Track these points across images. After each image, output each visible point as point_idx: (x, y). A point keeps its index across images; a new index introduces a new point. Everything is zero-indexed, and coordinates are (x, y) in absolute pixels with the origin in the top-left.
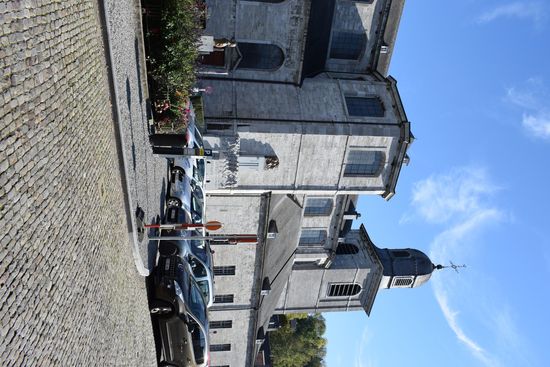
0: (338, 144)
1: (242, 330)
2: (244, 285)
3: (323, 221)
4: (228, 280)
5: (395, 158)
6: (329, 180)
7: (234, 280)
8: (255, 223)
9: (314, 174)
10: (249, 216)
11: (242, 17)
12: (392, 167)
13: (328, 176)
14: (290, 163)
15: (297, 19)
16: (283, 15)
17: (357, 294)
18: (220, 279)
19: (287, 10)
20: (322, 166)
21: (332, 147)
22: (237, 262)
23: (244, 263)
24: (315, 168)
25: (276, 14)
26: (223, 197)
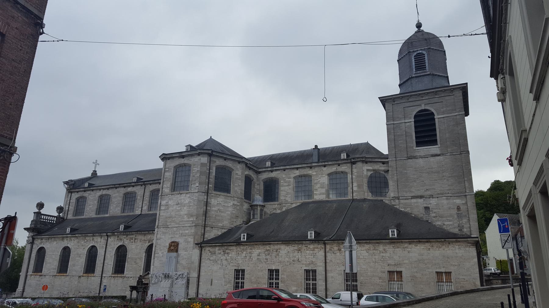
0: (167, 201)
1: (361, 257)
2: (292, 259)
3: (318, 180)
4: (285, 277)
5: (179, 158)
6: (191, 200)
7: (285, 270)
8: (225, 253)
9: (186, 213)
10: (218, 260)
11: (132, 273)
12: (185, 157)
13: (188, 202)
14: (176, 232)
15: (135, 239)
16: (133, 247)
17: (431, 111)
18: (283, 284)
19: (131, 246)
20: (180, 208)
21: (168, 205)
22: (263, 268)
23: (266, 261)
24: (181, 213)
25: (132, 252)
26: (200, 283)
